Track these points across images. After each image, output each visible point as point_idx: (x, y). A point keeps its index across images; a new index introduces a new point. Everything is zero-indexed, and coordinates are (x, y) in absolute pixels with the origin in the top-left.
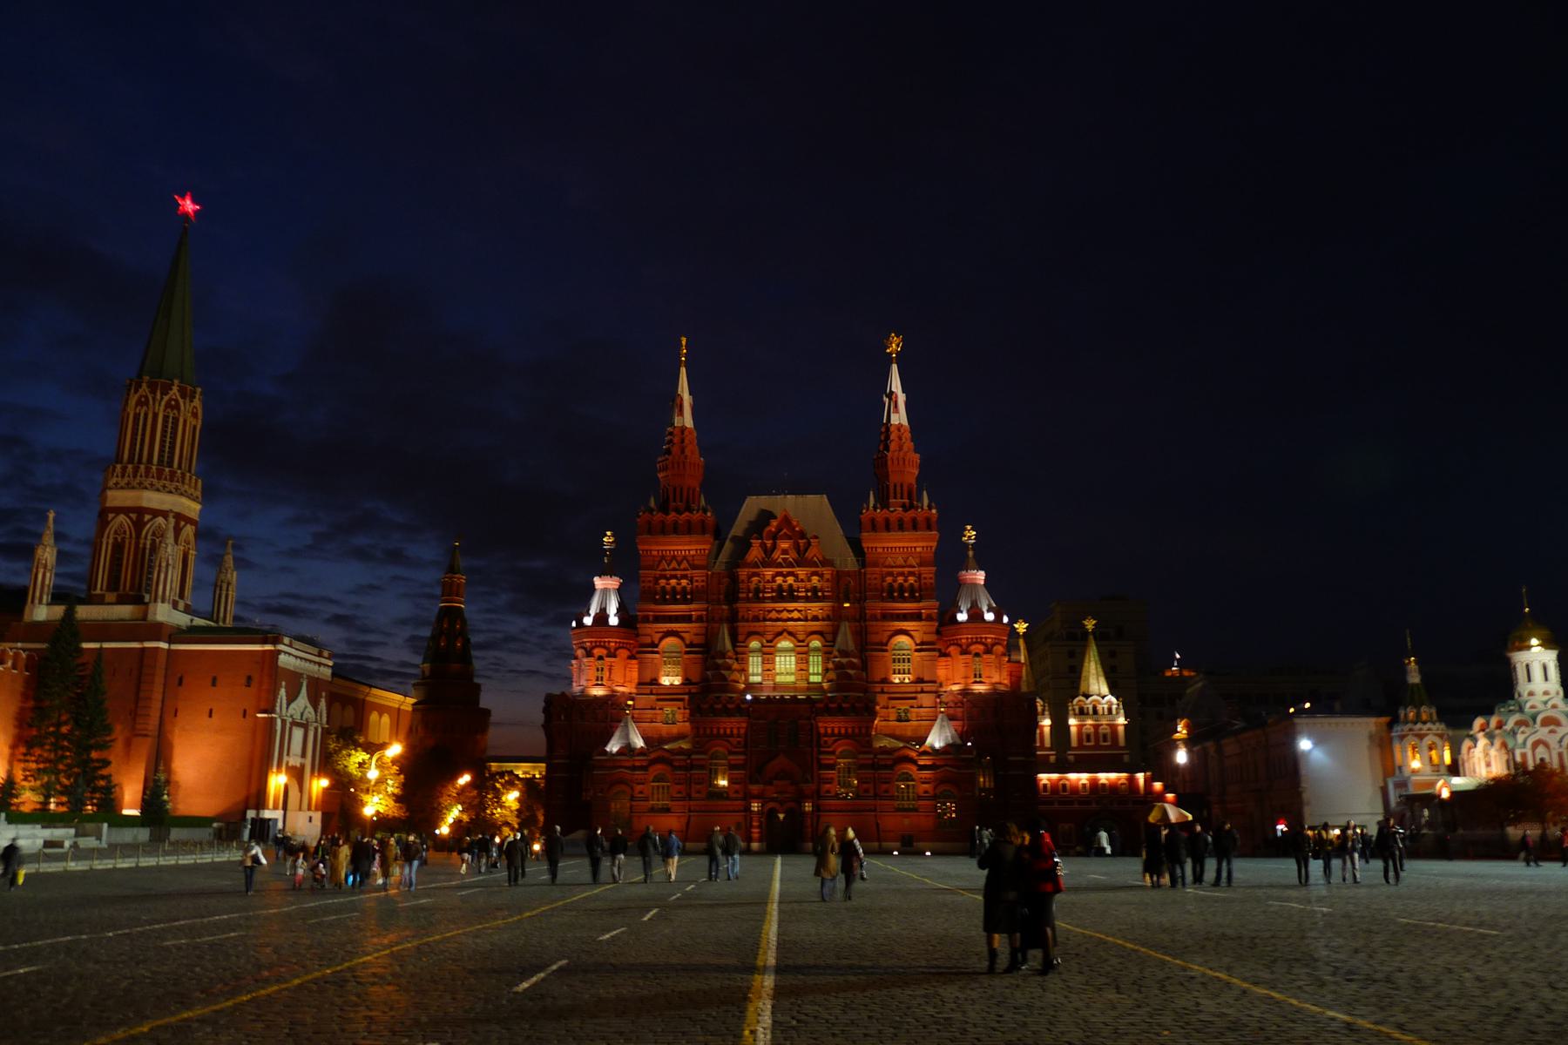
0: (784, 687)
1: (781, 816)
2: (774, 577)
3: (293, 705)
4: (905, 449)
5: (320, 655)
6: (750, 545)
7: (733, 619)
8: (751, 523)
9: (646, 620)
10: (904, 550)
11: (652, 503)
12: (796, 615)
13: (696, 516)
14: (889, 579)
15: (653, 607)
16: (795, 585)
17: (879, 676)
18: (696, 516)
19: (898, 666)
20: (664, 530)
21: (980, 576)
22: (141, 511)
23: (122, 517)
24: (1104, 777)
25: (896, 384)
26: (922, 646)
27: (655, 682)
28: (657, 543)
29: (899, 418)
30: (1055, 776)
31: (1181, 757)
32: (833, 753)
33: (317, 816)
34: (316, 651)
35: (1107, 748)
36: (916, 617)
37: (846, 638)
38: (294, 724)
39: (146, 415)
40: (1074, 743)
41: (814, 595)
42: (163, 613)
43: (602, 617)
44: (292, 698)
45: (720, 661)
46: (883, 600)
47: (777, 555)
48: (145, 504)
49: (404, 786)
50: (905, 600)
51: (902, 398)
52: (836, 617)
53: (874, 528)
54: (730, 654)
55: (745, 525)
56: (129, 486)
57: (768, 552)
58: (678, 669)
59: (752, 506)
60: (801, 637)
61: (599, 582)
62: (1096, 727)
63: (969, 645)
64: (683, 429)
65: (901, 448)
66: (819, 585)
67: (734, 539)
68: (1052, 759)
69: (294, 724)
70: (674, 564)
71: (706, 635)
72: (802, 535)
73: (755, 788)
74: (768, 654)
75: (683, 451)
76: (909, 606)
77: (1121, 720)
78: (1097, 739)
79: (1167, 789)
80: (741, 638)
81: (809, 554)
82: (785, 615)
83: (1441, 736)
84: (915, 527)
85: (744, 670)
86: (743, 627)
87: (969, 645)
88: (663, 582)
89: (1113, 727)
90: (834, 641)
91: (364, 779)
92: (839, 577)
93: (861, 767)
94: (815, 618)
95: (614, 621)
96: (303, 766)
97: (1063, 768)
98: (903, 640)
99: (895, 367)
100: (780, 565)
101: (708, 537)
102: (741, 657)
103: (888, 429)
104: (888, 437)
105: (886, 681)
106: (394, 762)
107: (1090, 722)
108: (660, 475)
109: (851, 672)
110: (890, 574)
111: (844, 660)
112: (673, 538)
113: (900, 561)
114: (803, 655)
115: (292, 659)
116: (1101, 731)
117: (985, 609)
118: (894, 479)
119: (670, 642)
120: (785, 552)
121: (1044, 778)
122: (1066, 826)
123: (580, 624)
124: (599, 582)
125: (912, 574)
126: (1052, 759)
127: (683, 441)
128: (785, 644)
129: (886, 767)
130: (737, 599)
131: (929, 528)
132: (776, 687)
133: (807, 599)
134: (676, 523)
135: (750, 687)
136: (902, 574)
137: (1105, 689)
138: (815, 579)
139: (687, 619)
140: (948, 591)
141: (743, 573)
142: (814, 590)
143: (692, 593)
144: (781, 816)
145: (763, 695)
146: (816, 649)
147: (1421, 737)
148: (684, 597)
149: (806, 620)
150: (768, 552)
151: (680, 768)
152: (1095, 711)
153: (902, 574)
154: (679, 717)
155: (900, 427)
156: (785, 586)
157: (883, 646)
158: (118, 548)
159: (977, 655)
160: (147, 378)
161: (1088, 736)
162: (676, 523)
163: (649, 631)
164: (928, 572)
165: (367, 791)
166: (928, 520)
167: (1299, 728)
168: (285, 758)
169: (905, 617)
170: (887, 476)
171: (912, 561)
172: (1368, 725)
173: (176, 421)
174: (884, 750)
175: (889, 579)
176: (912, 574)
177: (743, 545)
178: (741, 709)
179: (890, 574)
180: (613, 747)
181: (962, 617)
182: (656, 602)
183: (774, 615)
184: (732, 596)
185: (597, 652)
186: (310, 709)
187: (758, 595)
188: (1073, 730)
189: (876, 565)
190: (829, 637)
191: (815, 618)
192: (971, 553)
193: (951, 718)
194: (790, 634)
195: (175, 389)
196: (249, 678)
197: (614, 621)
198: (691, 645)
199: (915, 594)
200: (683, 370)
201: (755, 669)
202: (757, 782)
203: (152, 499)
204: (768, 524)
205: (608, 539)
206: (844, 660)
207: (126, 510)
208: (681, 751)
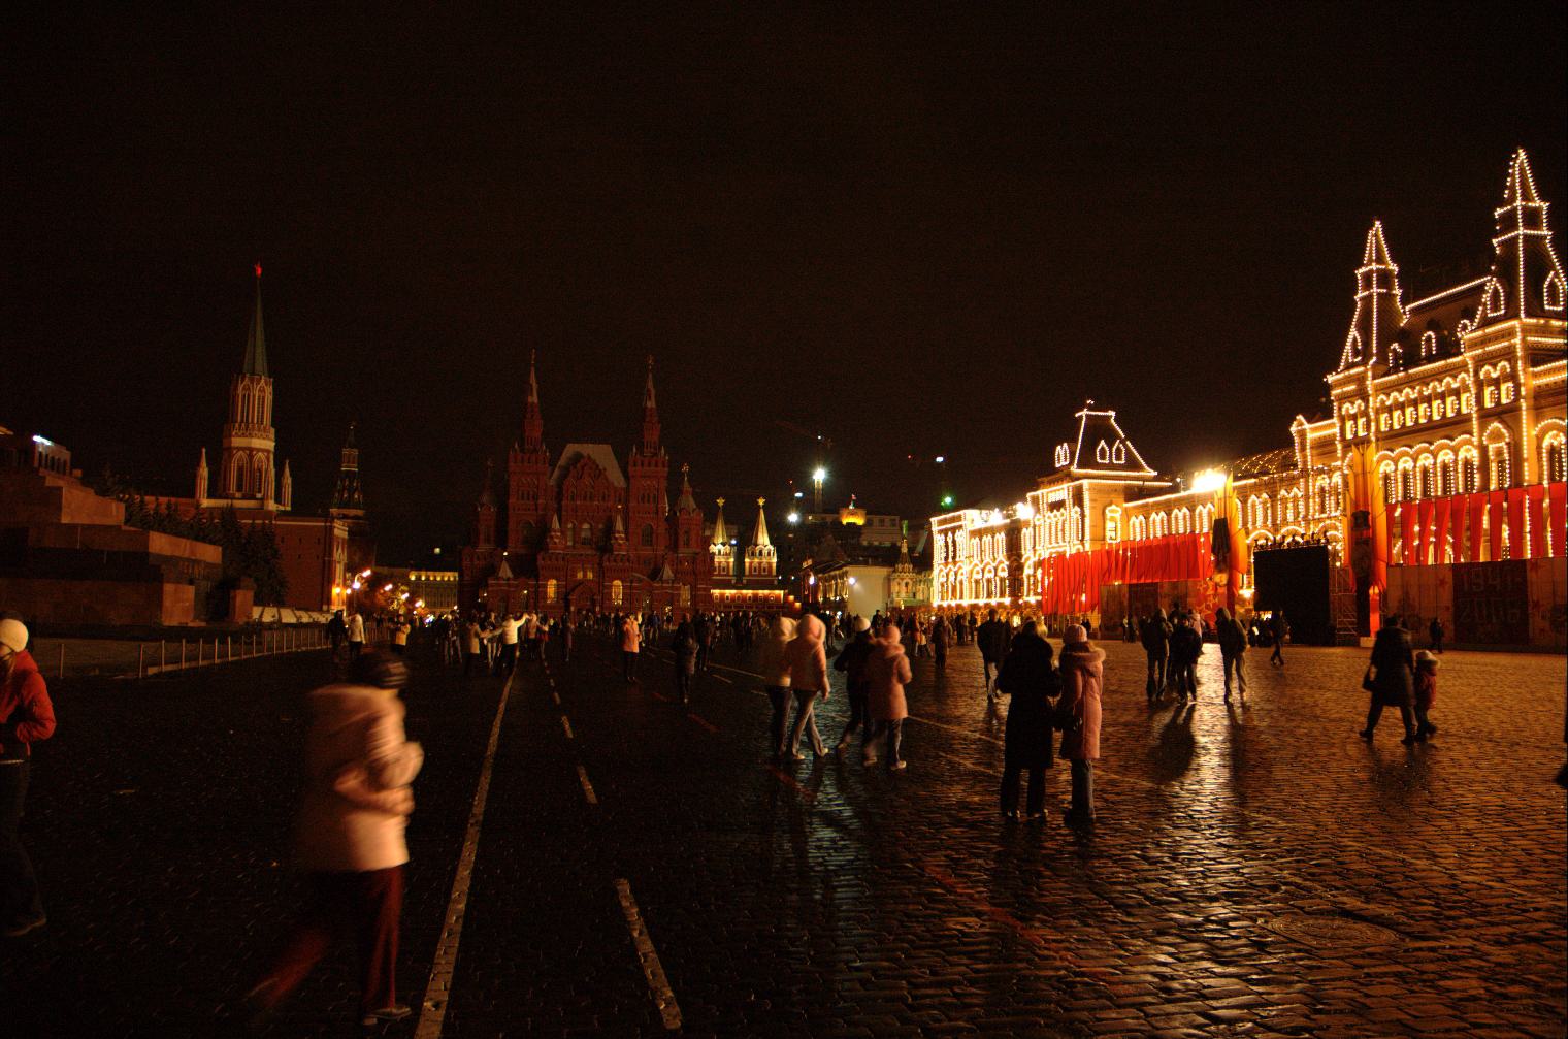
22: (251, 449)
23: (241, 452)
24: (762, 593)
25: (650, 384)
29: (651, 404)
30: (734, 592)
35: (765, 576)
39: (249, 395)
40: (747, 572)
42: (272, 505)
48: (253, 445)
56: (244, 435)
59: (571, 449)
62: (760, 564)
64: (533, 403)
68: (733, 582)
77: (774, 560)
78: (760, 571)
79: (796, 600)
83: (912, 579)
89: (770, 564)
107: (756, 560)
116: (762, 565)
121: (716, 592)
126: (733, 582)
147: (902, 579)
152: (761, 553)
158: (240, 469)
160: (248, 375)
172: (883, 571)
173: (264, 398)
188: (747, 565)
195: (263, 381)
203: (257, 443)
207: (243, 449)
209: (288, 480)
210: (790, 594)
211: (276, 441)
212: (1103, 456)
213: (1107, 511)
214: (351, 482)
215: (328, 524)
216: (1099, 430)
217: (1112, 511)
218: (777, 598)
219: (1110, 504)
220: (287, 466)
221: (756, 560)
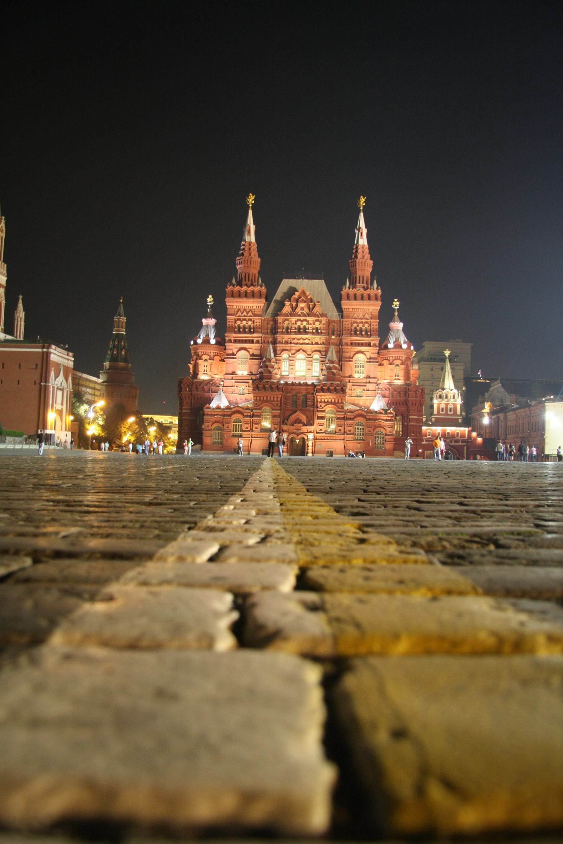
0: (300, 377)
1: (297, 441)
2: (296, 322)
3: (57, 380)
4: (366, 258)
5: (68, 355)
6: (284, 305)
7: (275, 342)
8: (284, 293)
9: (230, 341)
10: (364, 309)
11: (234, 281)
12: (307, 341)
13: (257, 289)
14: (355, 325)
15: (234, 335)
16: (307, 326)
17: (347, 373)
18: (257, 289)
19: (357, 369)
20: (240, 295)
21: (400, 326)
25: (362, 223)
26: (370, 360)
27: (233, 373)
28: (237, 302)
29: (363, 241)
31: (486, 421)
32: (324, 411)
33: (69, 434)
34: (66, 352)
35: (450, 415)
36: (369, 345)
37: (332, 354)
38: (58, 389)
40: (435, 412)
41: (317, 332)
43: (206, 341)
44: (57, 376)
45: (268, 363)
46: (351, 335)
47: (298, 310)
49: (106, 421)
50: (362, 335)
51: (365, 231)
52: (327, 343)
53: (348, 298)
54: (274, 360)
55: (282, 294)
57: (294, 309)
58: (247, 367)
59: (286, 284)
60: (309, 353)
61: (204, 321)
62: (447, 405)
63: (393, 360)
64: (250, 243)
65: (363, 257)
66: (319, 326)
67: (276, 301)
69: (58, 389)
70: (245, 313)
71: (261, 350)
72: (311, 301)
73: (285, 427)
74: (291, 359)
75: (250, 254)
76: (365, 339)
77: (459, 402)
80: (278, 352)
81: (315, 311)
82: (301, 341)
84: (369, 299)
86: (279, 347)
87: (393, 360)
88: (239, 322)
89: (455, 405)
90: (326, 355)
91: (86, 418)
92: (329, 323)
93: (338, 418)
94: (317, 343)
95: (213, 341)
96: (62, 409)
98: (360, 356)
99: (362, 215)
100: (299, 316)
101: (263, 300)
103: (357, 247)
104: (357, 251)
105: (350, 376)
106: (102, 409)
108: (238, 267)
109: (335, 371)
110: (356, 322)
111: (331, 365)
112: (244, 300)
113: (361, 316)
115: (56, 356)
116: (449, 407)
117: (402, 342)
118: (359, 273)
119: (242, 352)
120: (302, 309)
122: (429, 452)
123: (195, 343)
124: (204, 321)
125: (366, 323)
127: (250, 249)
128: (301, 355)
129: (350, 419)
130: (276, 333)
131: (376, 299)
133: (313, 333)
134: (246, 292)
135: (282, 377)
136: (362, 322)
137: (452, 386)
138: (317, 323)
139: (252, 342)
140: (384, 332)
141: (280, 319)
142: (317, 329)
143: (254, 328)
144: (297, 441)
145: (290, 381)
146: (317, 359)
148: (251, 330)
149: (312, 344)
150: (294, 309)
151: (247, 416)
153: (362, 322)
154: (246, 391)
155: (363, 247)
156: (302, 327)
157: (350, 359)
159: (397, 365)
161: (443, 409)
162: (246, 292)
163: (231, 347)
164: (375, 323)
165: (89, 423)
166: (376, 295)
167: (547, 408)
168: (55, 405)
169: (362, 345)
170: (356, 272)
171: (367, 316)
174: (351, 411)
175: (355, 325)
176: (366, 323)
177: (281, 305)
178: (278, 387)
179: (356, 322)
180: (213, 405)
181: (391, 346)
182: (235, 332)
183: (295, 341)
184: (274, 330)
185: (204, 357)
186: (65, 382)
187: (288, 331)
188: (435, 406)
189: (348, 317)
190: (324, 353)
191: (317, 343)
192: (396, 314)
193: (384, 396)
194: (304, 351)
196: (37, 365)
197: (213, 341)
198: (253, 355)
199: (368, 333)
200: (250, 212)
202: (286, 424)
204: (294, 294)
205: (210, 299)
206: (331, 365)
208: (248, 409)
209: (21, 314)
210: (473, 430)
211: (7, 276)
214: (119, 342)
215: (45, 350)
220: (20, 301)
221: (444, 402)
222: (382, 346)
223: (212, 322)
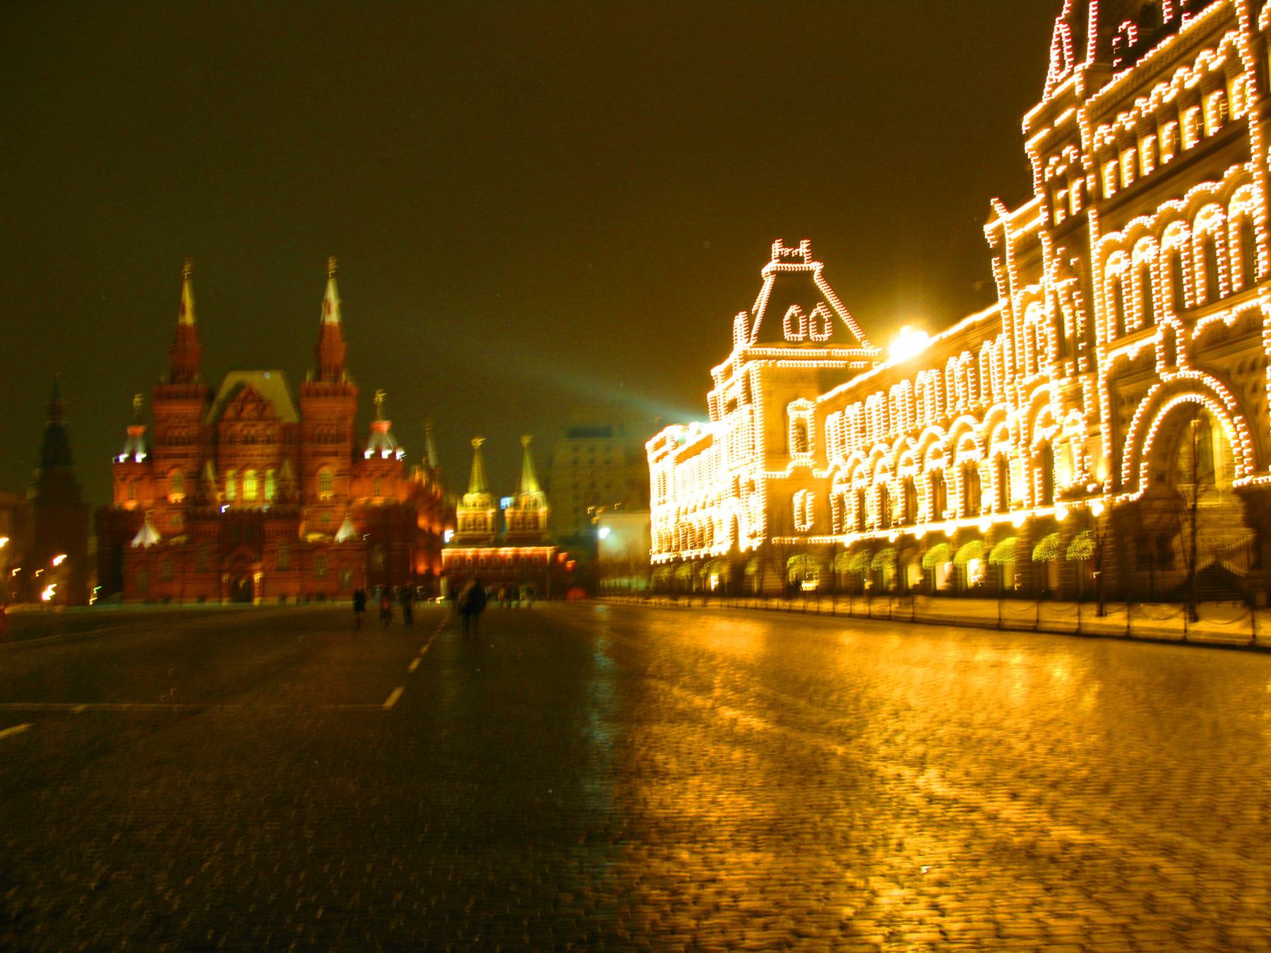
21: (385, 426)
25: (332, 294)
37: (288, 470)
41: (269, 441)
47: (245, 414)
52: (282, 455)
59: (232, 379)
74: (240, 479)
85: (222, 489)
89: (536, 519)
97: (499, 543)
102: (221, 482)
105: (314, 496)
114: (262, 479)
132: (243, 501)
148: (187, 442)
157: (313, 474)
178: (217, 516)
187: (232, 441)
199: (339, 438)
201: (231, 490)
212: (795, 329)
213: (789, 408)
216: (794, 289)
217: (798, 409)
218: (543, 557)
219: (795, 398)
222: (357, 454)
223: (140, 430)
